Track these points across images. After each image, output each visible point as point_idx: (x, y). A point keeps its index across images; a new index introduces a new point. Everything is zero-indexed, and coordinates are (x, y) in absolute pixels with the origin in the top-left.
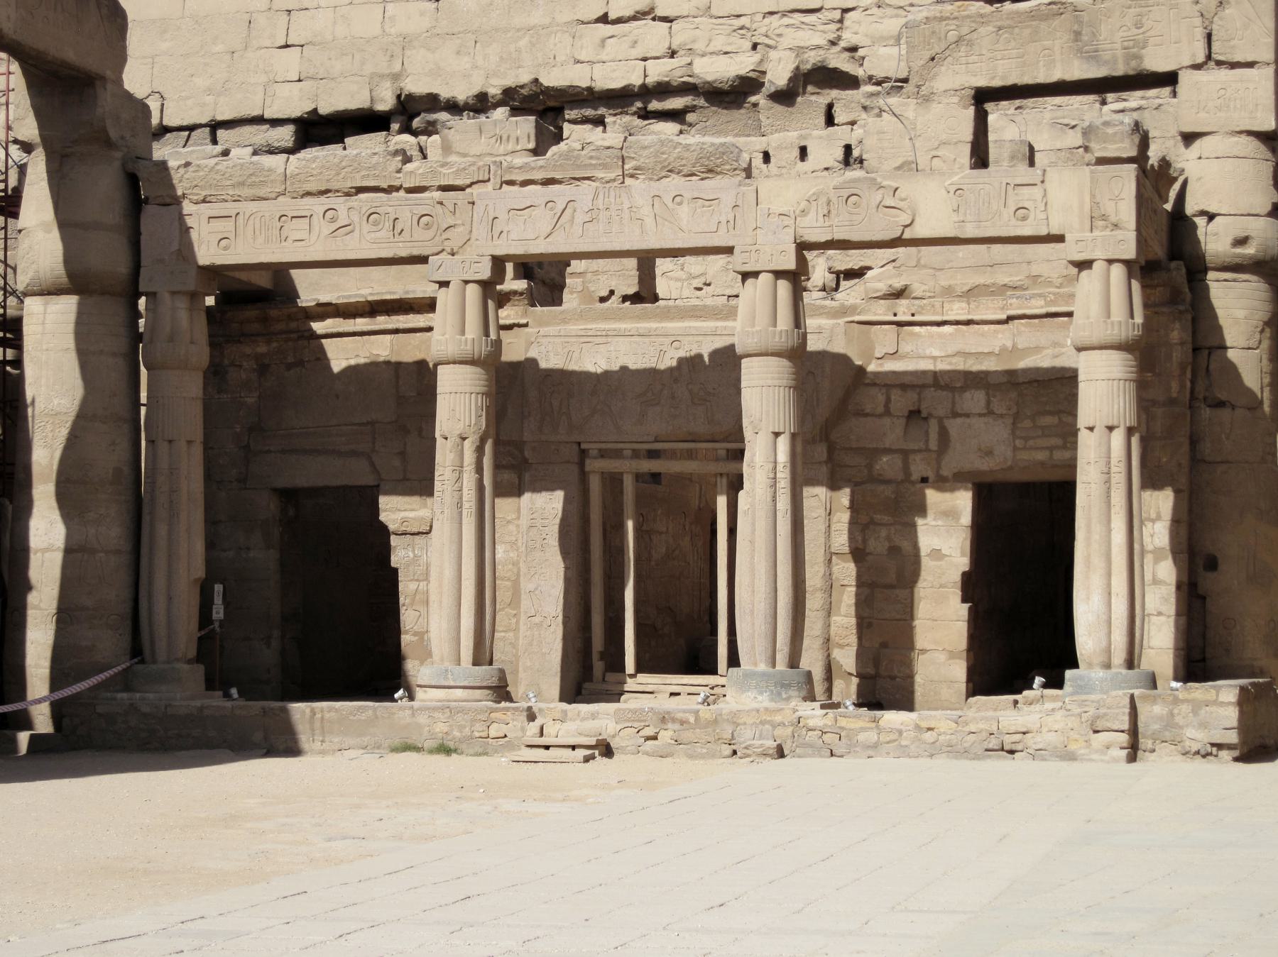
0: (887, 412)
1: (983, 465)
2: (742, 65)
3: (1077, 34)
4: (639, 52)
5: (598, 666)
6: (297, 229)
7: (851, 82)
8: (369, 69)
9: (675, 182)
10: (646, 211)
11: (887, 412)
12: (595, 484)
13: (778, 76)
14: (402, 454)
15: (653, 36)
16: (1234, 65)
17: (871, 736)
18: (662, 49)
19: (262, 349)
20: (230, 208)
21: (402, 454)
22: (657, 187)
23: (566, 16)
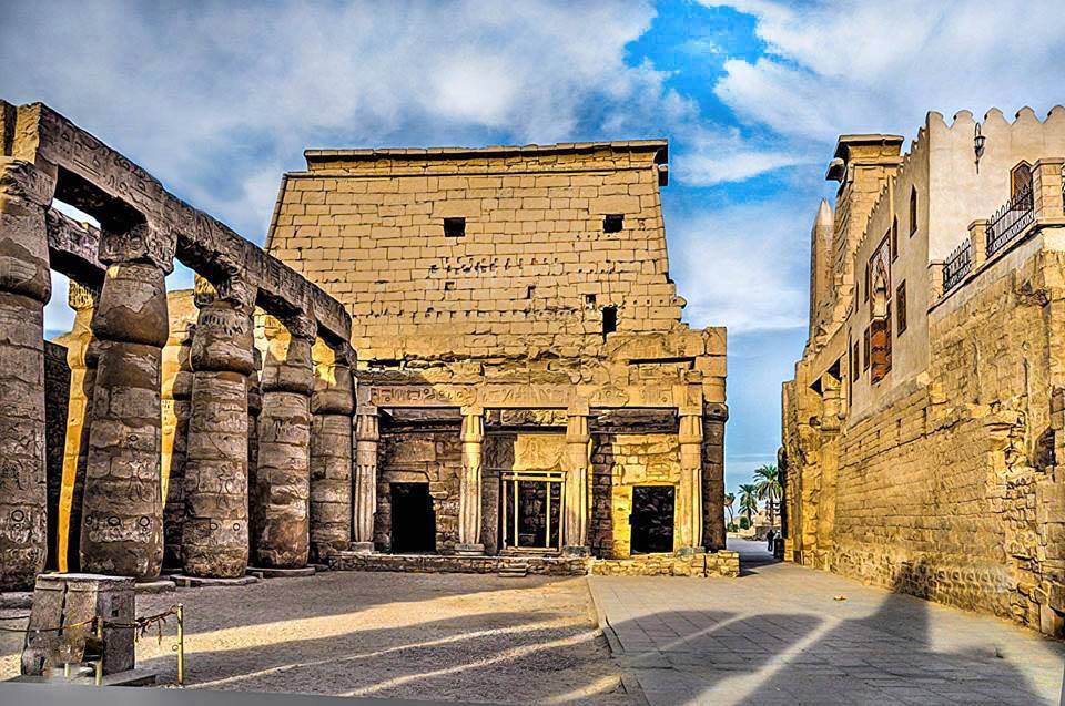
0: (605, 463)
1: (637, 480)
2: (522, 350)
3: (664, 344)
4: (487, 344)
5: (505, 544)
6: (414, 396)
7: (557, 357)
8: (394, 346)
9: (547, 386)
10: (538, 395)
11: (605, 463)
12: (505, 484)
13: (533, 353)
14: (437, 473)
15: (491, 340)
16: (713, 355)
17: (617, 569)
18: (494, 344)
19: (387, 436)
20: (390, 388)
21: (437, 473)
22: (541, 387)
23: (461, 332)
